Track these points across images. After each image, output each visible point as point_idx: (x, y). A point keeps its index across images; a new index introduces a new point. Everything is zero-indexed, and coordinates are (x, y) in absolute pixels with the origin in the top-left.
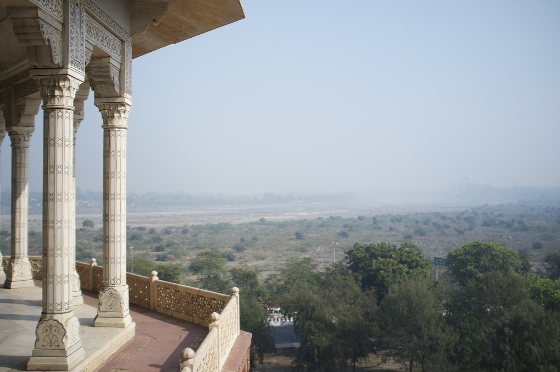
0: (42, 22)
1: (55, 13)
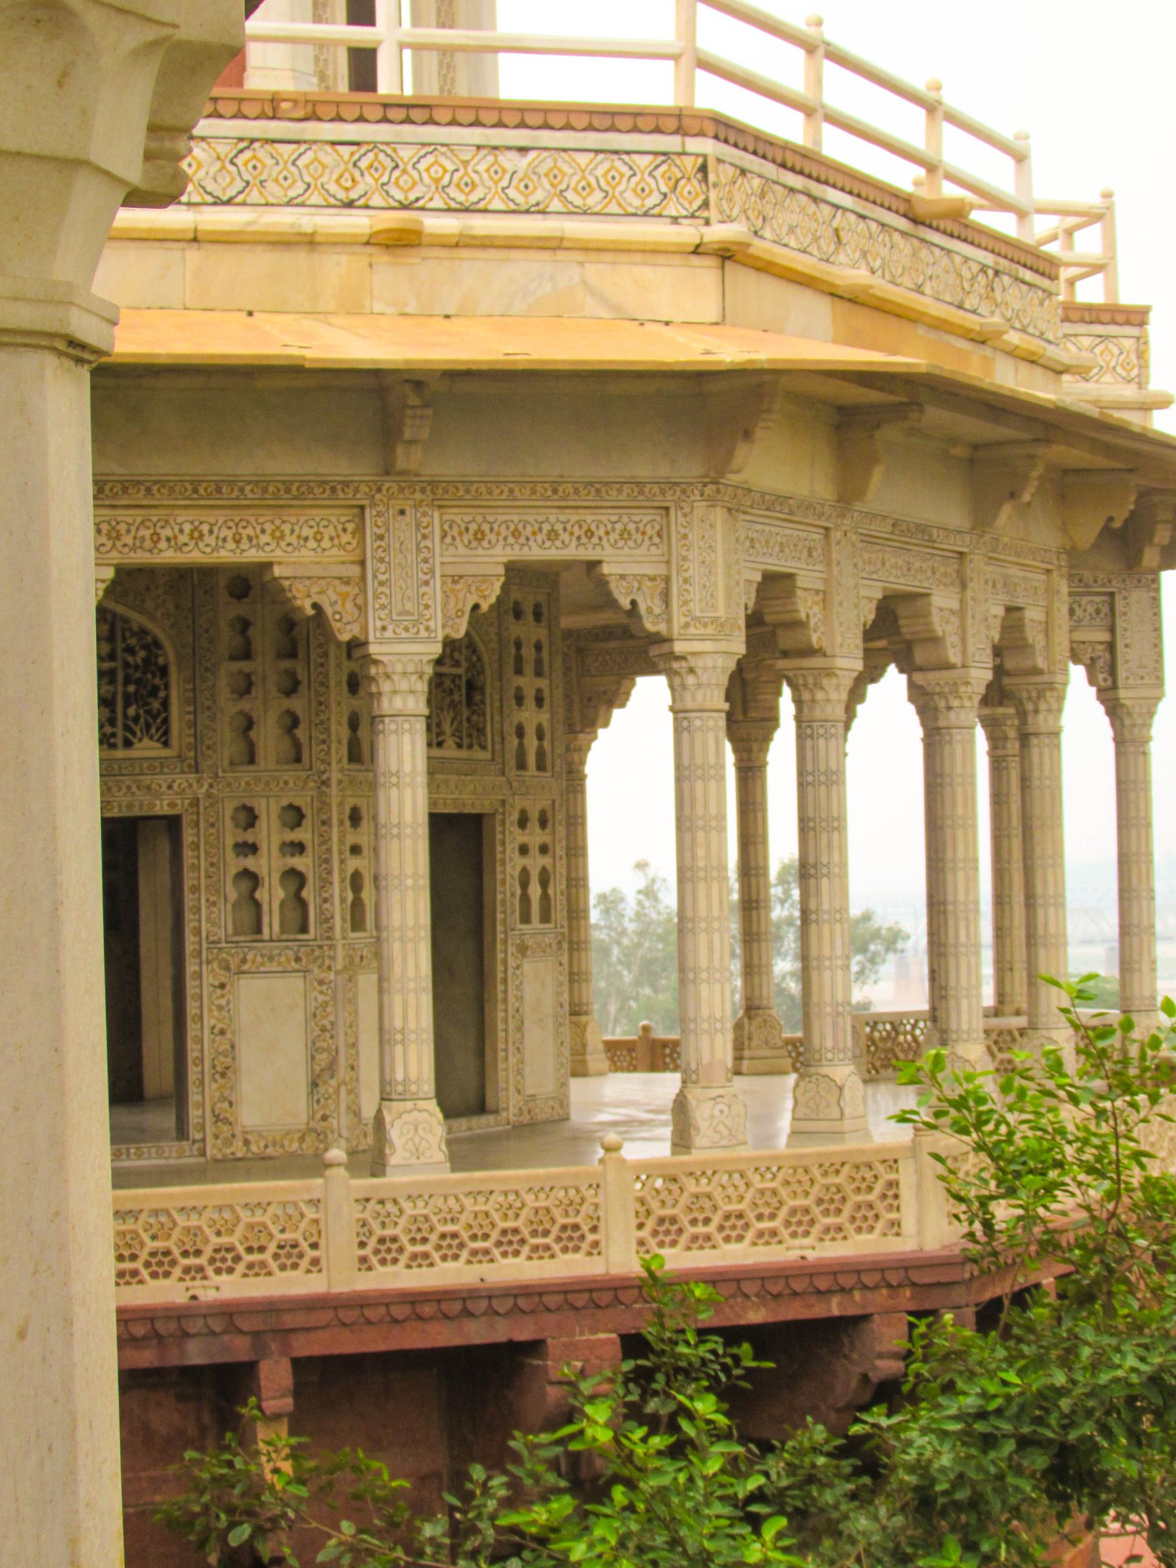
0: (286, 583)
1: (335, 551)
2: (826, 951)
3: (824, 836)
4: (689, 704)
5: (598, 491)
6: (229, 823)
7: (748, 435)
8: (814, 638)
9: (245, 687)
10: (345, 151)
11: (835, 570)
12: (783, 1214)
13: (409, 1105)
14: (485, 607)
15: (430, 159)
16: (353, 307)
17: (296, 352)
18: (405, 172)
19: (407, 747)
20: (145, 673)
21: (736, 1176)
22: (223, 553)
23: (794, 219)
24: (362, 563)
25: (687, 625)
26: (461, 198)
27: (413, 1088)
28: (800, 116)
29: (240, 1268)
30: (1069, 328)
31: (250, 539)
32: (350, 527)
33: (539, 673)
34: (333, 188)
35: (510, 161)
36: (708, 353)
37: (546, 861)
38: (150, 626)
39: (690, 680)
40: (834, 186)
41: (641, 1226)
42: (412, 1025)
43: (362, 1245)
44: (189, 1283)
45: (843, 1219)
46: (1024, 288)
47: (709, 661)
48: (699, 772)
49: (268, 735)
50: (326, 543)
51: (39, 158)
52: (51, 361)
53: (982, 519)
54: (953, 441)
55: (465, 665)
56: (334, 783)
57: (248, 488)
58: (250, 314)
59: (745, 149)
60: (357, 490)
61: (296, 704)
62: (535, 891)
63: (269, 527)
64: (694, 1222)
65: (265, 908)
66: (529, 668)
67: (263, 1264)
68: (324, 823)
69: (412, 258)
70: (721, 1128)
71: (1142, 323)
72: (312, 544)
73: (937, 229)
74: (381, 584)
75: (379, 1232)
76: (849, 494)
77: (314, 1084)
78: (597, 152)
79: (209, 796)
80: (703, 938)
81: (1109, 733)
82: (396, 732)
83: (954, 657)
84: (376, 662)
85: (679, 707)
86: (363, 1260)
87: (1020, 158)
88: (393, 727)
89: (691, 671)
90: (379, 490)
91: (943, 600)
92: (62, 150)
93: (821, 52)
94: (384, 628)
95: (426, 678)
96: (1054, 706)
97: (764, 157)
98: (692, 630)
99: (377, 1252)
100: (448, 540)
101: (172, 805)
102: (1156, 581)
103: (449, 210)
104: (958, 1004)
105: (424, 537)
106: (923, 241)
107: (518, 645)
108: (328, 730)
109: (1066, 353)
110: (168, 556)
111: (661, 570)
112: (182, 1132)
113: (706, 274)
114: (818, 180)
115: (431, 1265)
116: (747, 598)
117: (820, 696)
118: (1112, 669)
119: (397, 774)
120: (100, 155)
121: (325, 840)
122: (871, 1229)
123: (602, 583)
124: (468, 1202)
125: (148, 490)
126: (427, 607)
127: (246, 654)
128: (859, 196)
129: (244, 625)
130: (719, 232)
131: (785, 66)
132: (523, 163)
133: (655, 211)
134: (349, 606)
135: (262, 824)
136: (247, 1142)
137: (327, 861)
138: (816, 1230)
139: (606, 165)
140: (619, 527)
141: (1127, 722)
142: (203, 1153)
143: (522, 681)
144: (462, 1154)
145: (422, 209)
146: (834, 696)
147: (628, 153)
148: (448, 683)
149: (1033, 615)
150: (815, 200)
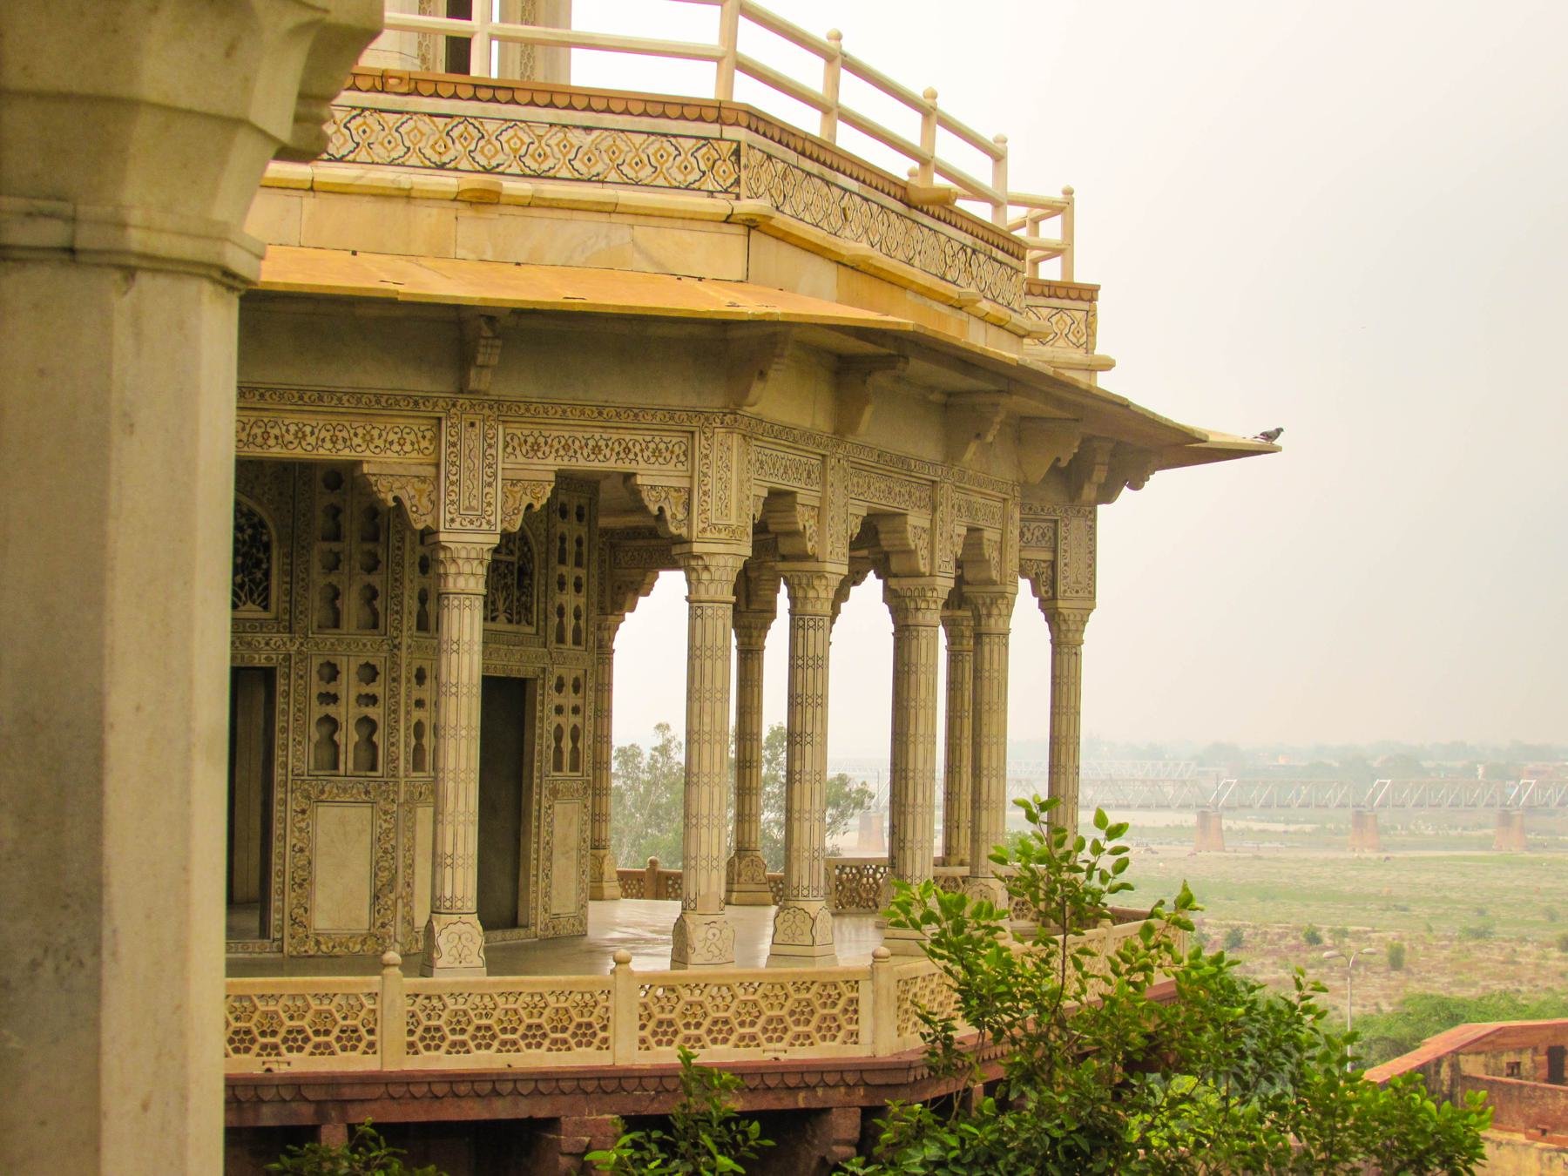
0: (373, 479)
1: (414, 454)
2: (807, 806)
3: (810, 710)
4: (704, 597)
5: (636, 415)
6: (314, 674)
7: (762, 375)
8: (809, 545)
9: (333, 565)
10: (440, 122)
11: (829, 490)
12: (761, 1022)
13: (455, 918)
14: (537, 507)
15: (511, 132)
16: (441, 252)
17: (392, 287)
18: (489, 142)
19: (467, 621)
20: (251, 547)
21: (724, 989)
22: (321, 451)
23: (809, 198)
24: (437, 465)
25: (704, 530)
26: (534, 166)
27: (459, 904)
28: (818, 114)
29: (309, 1047)
30: (1030, 300)
31: (344, 440)
32: (429, 434)
33: (578, 564)
34: (428, 152)
35: (576, 137)
36: (733, 305)
37: (578, 720)
38: (258, 509)
39: (705, 576)
40: (844, 173)
41: (643, 1027)
42: (460, 851)
43: (411, 1033)
44: (265, 1058)
45: (811, 1028)
46: (997, 265)
47: (721, 561)
48: (708, 653)
49: (351, 605)
50: (408, 447)
51: (206, 116)
52: (207, 288)
53: (952, 455)
54: (932, 389)
55: (517, 554)
56: (404, 648)
57: (345, 398)
58: (354, 253)
59: (772, 139)
60: (435, 404)
61: (376, 580)
62: (567, 744)
63: (360, 431)
64: (687, 1025)
65: (342, 748)
66: (571, 559)
67: (328, 1045)
68: (394, 680)
69: (491, 213)
70: (713, 948)
71: (1092, 300)
72: (396, 447)
73: (927, 213)
74: (452, 483)
75: (426, 1023)
76: (844, 427)
77: (376, 897)
78: (649, 134)
79: (299, 652)
80: (705, 790)
81: (1048, 636)
82: (458, 607)
83: (923, 567)
84: (445, 548)
85: (694, 597)
86: (411, 1045)
87: (998, 158)
88: (456, 603)
89: (706, 568)
90: (454, 405)
91: (917, 519)
92: (225, 109)
93: (838, 62)
94: (452, 520)
95: (486, 563)
96: (1004, 612)
97: (787, 146)
98: (708, 535)
99: (423, 1039)
100: (509, 450)
101: (268, 659)
102: (1094, 512)
103: (524, 176)
104: (913, 855)
105: (490, 446)
106: (914, 221)
107: (563, 539)
108: (401, 603)
109: (1027, 321)
110: (276, 451)
111: (685, 483)
112: (264, 932)
113: (734, 240)
114: (831, 167)
115: (468, 1052)
116: (754, 509)
117: (811, 594)
118: (1053, 584)
119: (457, 642)
120: (258, 117)
121: (394, 695)
122: (835, 1037)
123: (635, 492)
124: (501, 1001)
125: (262, 395)
126: (489, 504)
127: (336, 536)
128: (864, 182)
129: (335, 512)
130: (747, 206)
131: (808, 71)
132: (588, 140)
133: (696, 185)
134: (425, 500)
135: (343, 677)
136: (318, 943)
137: (395, 712)
138: (788, 1037)
139: (657, 145)
140: (652, 445)
141: (1064, 627)
142: (282, 951)
143: (563, 570)
144: (497, 961)
145: (502, 173)
146: (823, 595)
147: (675, 136)
148: (502, 568)
149: (991, 535)
150: (827, 183)
